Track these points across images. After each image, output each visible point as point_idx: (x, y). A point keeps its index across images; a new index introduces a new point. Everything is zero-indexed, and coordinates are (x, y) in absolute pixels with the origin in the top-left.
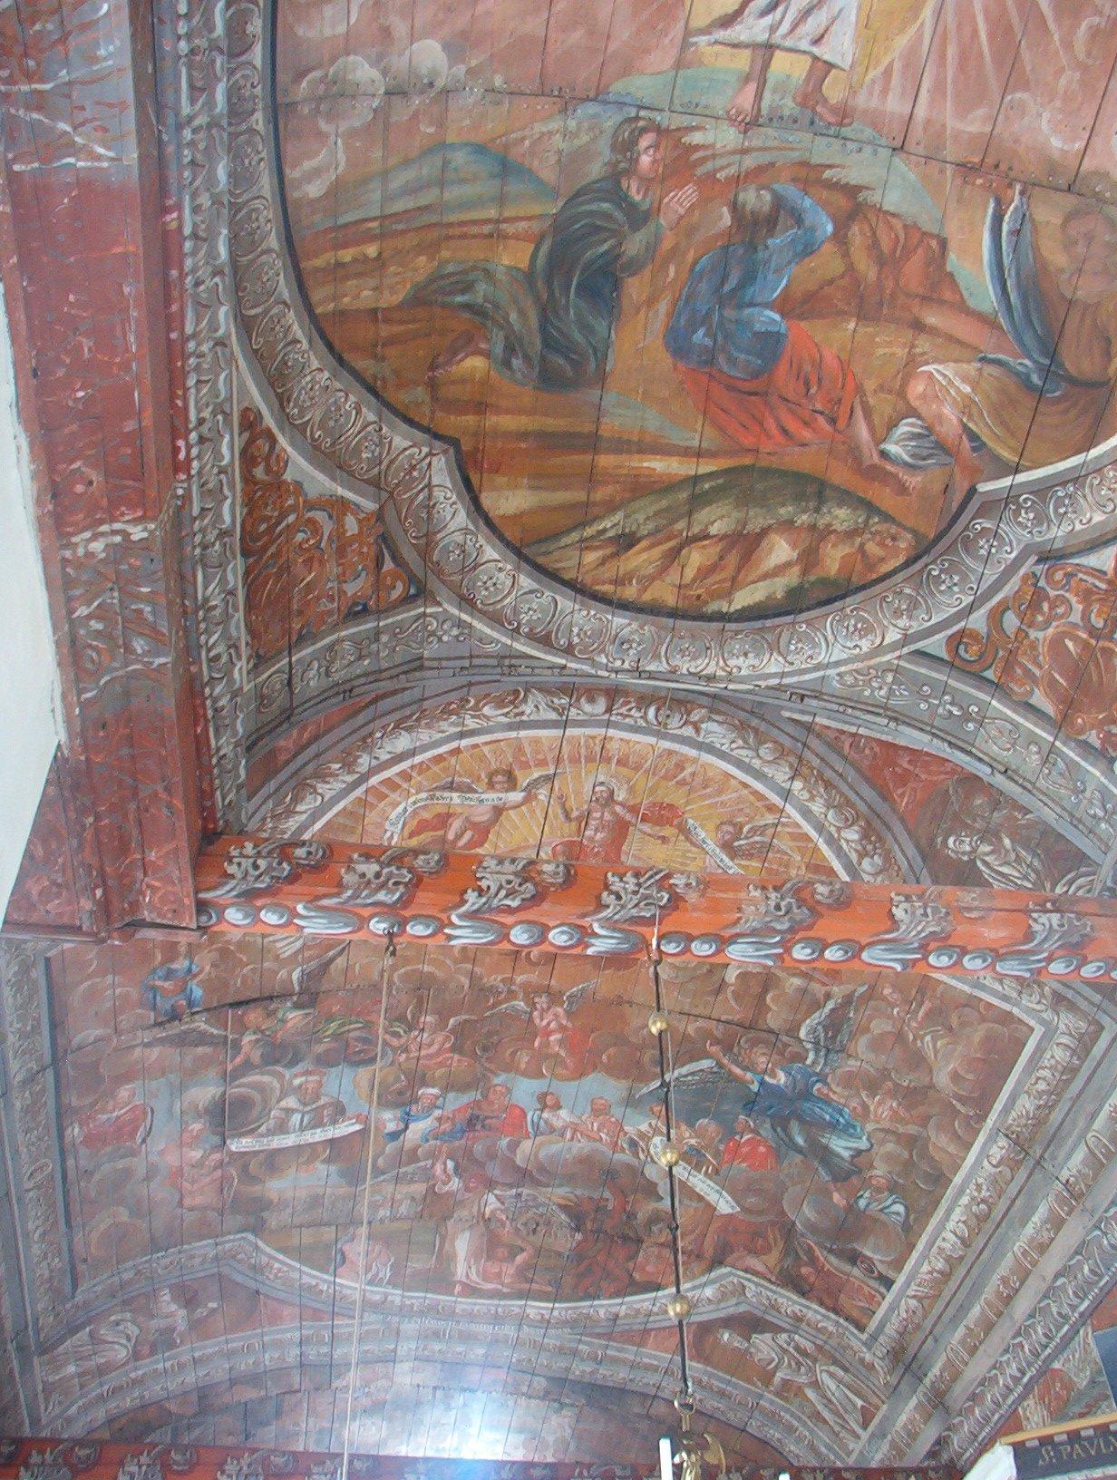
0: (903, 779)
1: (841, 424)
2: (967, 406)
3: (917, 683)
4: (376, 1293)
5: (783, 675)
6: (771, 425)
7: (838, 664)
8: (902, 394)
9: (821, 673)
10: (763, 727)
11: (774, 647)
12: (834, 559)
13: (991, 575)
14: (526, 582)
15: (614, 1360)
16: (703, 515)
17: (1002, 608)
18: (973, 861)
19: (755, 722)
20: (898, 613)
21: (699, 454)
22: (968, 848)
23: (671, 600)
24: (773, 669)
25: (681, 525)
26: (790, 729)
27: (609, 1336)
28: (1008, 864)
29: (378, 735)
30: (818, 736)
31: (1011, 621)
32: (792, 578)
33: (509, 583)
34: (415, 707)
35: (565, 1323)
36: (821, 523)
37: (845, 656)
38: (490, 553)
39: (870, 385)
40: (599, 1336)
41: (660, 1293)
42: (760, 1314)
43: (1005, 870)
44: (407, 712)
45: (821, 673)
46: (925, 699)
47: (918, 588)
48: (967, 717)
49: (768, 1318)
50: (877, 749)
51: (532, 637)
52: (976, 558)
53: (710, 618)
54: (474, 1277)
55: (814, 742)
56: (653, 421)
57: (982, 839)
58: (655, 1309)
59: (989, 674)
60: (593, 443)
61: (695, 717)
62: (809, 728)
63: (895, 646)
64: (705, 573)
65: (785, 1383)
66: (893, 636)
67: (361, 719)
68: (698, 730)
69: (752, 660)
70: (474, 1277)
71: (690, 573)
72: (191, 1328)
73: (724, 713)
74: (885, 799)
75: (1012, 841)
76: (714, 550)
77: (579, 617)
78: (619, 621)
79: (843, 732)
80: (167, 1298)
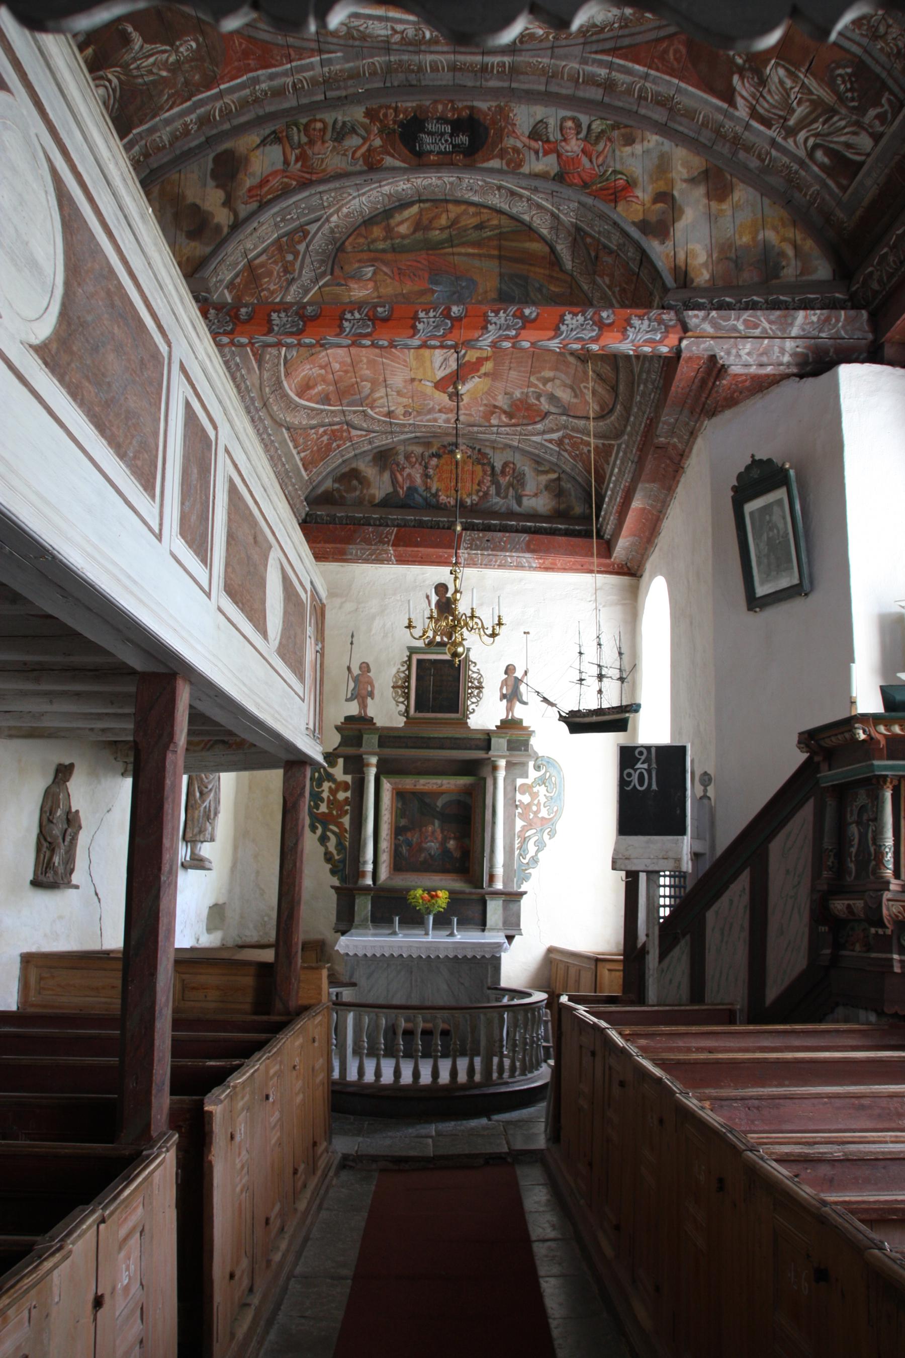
0: (246, 54)
1: (395, 269)
2: (350, 290)
3: (312, 210)
5: (380, 186)
6: (425, 263)
7: (354, 198)
8: (375, 282)
9: (361, 192)
10: (351, 42)
11: (390, 196)
12: (377, 232)
13: (308, 260)
14: (526, 218)
16: (445, 235)
17: (296, 258)
18: (172, 45)
19: (357, 43)
20: (337, 226)
21: (453, 254)
22: (181, 49)
23: (451, 207)
24: (387, 188)
25: (454, 233)
26: (332, 47)
28: (154, 64)
29: (616, 25)
30: (312, 50)
31: (290, 257)
32: (393, 222)
33: (534, 219)
34: (590, 40)
36: (389, 241)
37: (352, 202)
38: (545, 232)
39: (389, 281)
43: (152, 60)
44: (594, 38)
45: (361, 192)
46: (304, 209)
47: (334, 238)
48: (283, 220)
50: (273, 62)
51: (521, 196)
52: (316, 261)
53: (427, 201)
55: (314, 45)
56: (476, 263)
57: (178, 61)
59: (285, 239)
60: (500, 258)
61: (397, 38)
62: (320, 52)
63: (331, 215)
64: (437, 217)
66: (334, 218)
67: (626, 42)
68: (393, 29)
69: (400, 189)
71: (444, 216)
73: (378, 42)
74: (250, 37)
75: (163, 77)
76: (436, 224)
77: (495, 200)
78: (476, 199)
79: (300, 59)
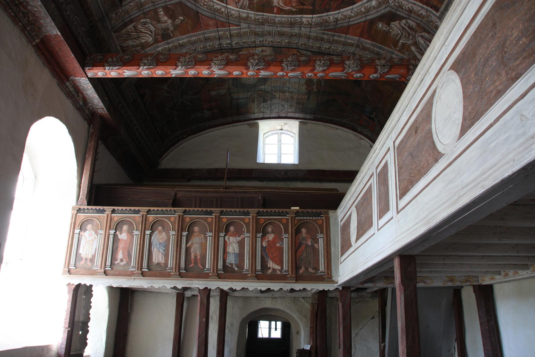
4: (244, 13)
15: (337, 42)
27: (334, 30)
35: (317, 25)
40: (330, 30)
41: (354, 6)
42: (394, 11)
49: (398, 13)
54: (281, 4)
58: (352, 15)
65: (403, 44)
70: (281, 4)
72: (175, 29)
80: (162, 13)
